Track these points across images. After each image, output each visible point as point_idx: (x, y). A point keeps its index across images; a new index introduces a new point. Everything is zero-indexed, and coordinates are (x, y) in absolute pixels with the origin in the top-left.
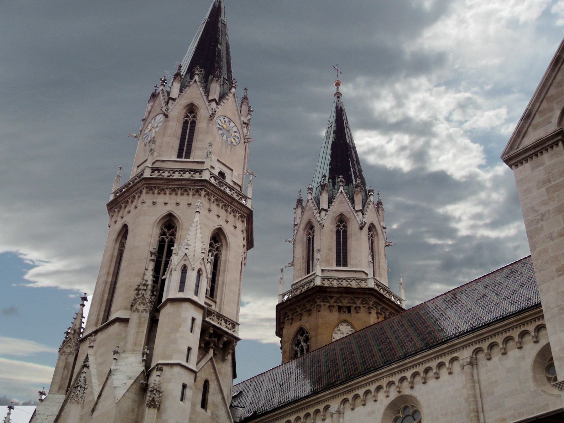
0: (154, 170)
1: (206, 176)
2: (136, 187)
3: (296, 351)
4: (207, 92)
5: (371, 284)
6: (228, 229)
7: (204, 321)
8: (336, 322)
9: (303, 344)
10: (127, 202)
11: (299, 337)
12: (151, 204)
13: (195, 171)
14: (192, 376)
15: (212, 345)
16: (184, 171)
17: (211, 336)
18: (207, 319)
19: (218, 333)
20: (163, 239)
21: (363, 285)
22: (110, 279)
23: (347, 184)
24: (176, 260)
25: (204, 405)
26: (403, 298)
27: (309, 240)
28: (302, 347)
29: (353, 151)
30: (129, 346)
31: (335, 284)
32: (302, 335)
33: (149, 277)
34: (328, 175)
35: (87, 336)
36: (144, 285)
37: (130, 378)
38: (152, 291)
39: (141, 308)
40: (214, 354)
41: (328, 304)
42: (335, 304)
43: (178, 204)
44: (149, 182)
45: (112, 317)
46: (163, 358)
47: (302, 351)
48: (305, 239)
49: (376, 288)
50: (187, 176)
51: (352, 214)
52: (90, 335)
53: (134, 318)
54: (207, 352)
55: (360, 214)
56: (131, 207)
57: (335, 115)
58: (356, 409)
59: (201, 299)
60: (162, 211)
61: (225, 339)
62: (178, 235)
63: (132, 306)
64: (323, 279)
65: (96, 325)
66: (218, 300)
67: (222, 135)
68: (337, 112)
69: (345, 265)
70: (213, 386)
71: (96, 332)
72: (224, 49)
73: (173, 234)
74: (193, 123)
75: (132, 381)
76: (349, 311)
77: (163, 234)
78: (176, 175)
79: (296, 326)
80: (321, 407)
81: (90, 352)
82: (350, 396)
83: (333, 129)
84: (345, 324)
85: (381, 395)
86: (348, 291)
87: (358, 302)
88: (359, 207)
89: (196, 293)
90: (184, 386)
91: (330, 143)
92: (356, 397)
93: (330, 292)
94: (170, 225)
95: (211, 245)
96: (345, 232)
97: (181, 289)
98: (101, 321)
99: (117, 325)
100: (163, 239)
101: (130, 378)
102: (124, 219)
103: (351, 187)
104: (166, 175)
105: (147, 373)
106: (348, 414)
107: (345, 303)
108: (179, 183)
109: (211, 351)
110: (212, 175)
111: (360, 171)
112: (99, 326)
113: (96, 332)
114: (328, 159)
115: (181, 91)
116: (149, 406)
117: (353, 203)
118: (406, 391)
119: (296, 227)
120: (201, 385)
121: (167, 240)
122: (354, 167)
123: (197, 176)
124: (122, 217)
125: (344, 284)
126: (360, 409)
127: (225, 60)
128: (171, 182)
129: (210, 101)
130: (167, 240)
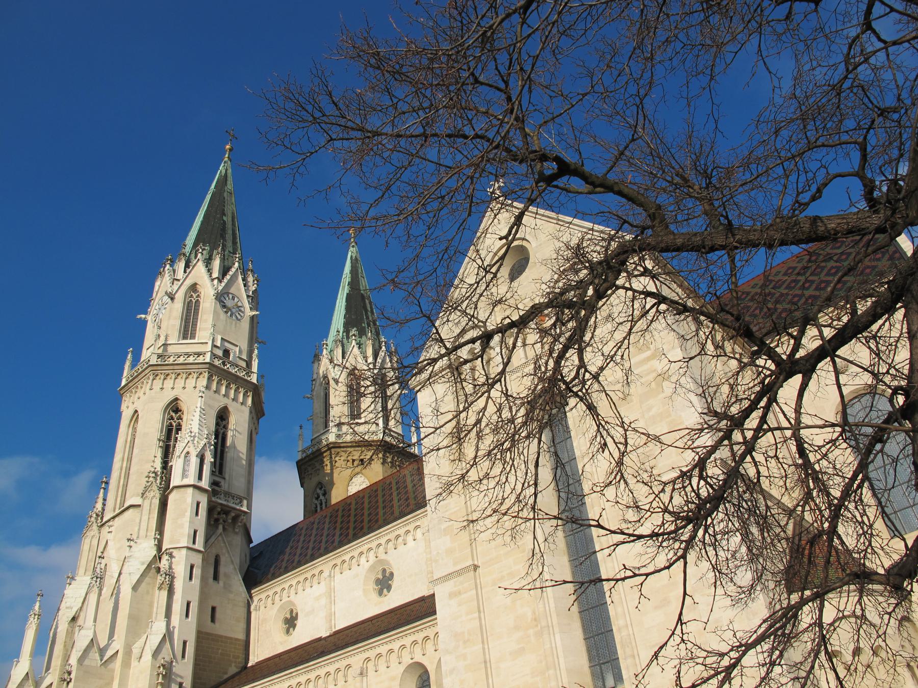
0: (159, 356)
1: (208, 360)
4: (210, 271)
6: (233, 407)
7: (209, 502)
9: (322, 497)
10: (137, 387)
11: (318, 491)
12: (159, 390)
13: (199, 354)
14: (200, 556)
15: (221, 521)
16: (188, 355)
17: (219, 513)
18: (213, 499)
19: (226, 511)
23: (360, 337)
24: (180, 446)
25: (216, 577)
30: (143, 532)
33: (158, 466)
34: (341, 330)
35: (106, 522)
36: (154, 472)
37: (143, 564)
38: (162, 478)
39: (152, 494)
40: (224, 529)
41: (342, 458)
42: (349, 458)
43: (184, 388)
44: (155, 368)
45: (127, 505)
46: (171, 542)
47: (321, 504)
48: (322, 394)
50: (191, 359)
52: (109, 520)
54: (217, 528)
56: (140, 393)
59: (205, 483)
60: (168, 396)
61: (233, 514)
62: (184, 419)
63: (143, 494)
65: (114, 511)
66: (227, 477)
67: (227, 312)
70: (223, 560)
71: (114, 518)
72: (230, 219)
73: (180, 418)
74: (198, 302)
78: (181, 360)
79: (315, 480)
80: (316, 572)
81: (110, 536)
82: (338, 561)
85: (363, 559)
89: (200, 478)
90: (192, 567)
92: (344, 562)
93: (344, 447)
95: (217, 424)
98: (118, 506)
99: (131, 510)
100: (171, 425)
102: (135, 405)
103: (364, 338)
105: (158, 557)
106: (338, 576)
107: (356, 455)
109: (221, 527)
110: (214, 356)
112: (117, 511)
113: (114, 518)
114: (343, 312)
115: (185, 272)
116: (160, 588)
118: (382, 556)
120: (212, 561)
122: (367, 318)
123: (200, 359)
126: (347, 573)
127: (230, 232)
128: (176, 367)
129: (213, 280)
130: (174, 424)
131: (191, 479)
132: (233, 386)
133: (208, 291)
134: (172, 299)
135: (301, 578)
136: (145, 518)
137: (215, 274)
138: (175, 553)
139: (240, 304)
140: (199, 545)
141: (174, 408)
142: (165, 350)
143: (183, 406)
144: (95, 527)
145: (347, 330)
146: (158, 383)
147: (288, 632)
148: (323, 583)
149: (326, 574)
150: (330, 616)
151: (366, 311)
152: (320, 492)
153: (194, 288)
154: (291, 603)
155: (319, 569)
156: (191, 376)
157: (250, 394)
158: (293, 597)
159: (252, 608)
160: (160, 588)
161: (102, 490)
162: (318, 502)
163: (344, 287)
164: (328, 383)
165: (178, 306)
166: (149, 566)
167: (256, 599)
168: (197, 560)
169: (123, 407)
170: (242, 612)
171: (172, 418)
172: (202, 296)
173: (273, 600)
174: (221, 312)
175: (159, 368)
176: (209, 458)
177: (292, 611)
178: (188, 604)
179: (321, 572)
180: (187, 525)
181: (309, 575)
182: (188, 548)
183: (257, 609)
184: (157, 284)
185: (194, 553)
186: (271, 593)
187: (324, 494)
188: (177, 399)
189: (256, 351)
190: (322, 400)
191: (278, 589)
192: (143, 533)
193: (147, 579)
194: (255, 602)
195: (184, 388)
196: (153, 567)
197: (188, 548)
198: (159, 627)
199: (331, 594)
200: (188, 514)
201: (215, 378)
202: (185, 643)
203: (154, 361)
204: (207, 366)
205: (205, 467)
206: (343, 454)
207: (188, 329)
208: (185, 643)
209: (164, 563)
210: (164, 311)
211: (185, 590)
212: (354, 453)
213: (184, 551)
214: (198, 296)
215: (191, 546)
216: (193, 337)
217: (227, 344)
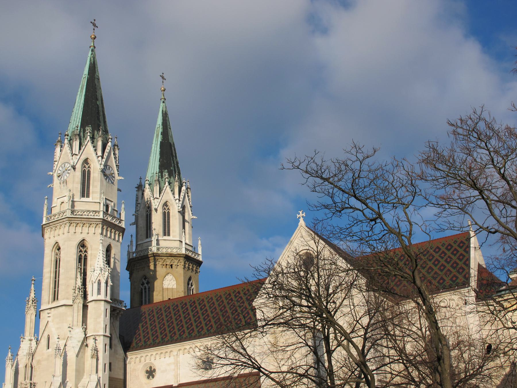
0: (73, 212)
1: (101, 217)
2: (62, 221)
3: (142, 289)
5: (183, 252)
6: (114, 244)
8: (165, 274)
11: (144, 281)
13: (96, 212)
20: (81, 255)
21: (179, 252)
22: (52, 275)
23: (170, 178)
26: (200, 252)
27: (147, 215)
28: (145, 287)
29: (173, 148)
30: (75, 323)
31: (164, 251)
32: (145, 279)
37: (79, 342)
41: (160, 263)
43: (88, 233)
44: (70, 219)
47: (145, 289)
48: (145, 215)
49: (187, 253)
50: (91, 215)
51: (174, 201)
53: (75, 306)
55: (177, 201)
57: (162, 118)
58: (185, 355)
59: (108, 299)
62: (89, 252)
64: (158, 249)
68: (163, 116)
69: (169, 235)
73: (86, 251)
74: (89, 172)
75: (80, 343)
76: (172, 267)
77: (81, 251)
80: (169, 350)
81: (49, 319)
82: (183, 348)
83: (161, 130)
84: (169, 275)
86: (171, 255)
87: (176, 261)
88: (177, 196)
91: (159, 143)
92: (185, 349)
94: (84, 245)
96: (169, 213)
97: (99, 293)
98: (51, 301)
99: (64, 307)
100: (81, 255)
101: (79, 342)
103: (172, 179)
104: (79, 213)
105: (86, 338)
106: (181, 355)
108: (88, 220)
111: (177, 163)
114: (158, 156)
115: (80, 149)
117: (173, 194)
119: (139, 205)
121: (83, 255)
122: (174, 162)
124: (54, 237)
125: (169, 251)
128: (83, 220)
129: (98, 157)
130: (83, 255)
131: (102, 297)
132: (113, 231)
133: (96, 166)
134: (74, 168)
135: (159, 352)
136: (76, 314)
137: (100, 153)
138: (97, 338)
139: (112, 172)
140: (108, 334)
141: (82, 245)
142: (73, 206)
143: (88, 244)
144: (32, 308)
145: (161, 172)
146: (72, 229)
147: (148, 378)
148: (172, 357)
149: (175, 353)
150: (177, 376)
151: (173, 156)
152: (145, 282)
153: (86, 161)
154: (153, 364)
155: (170, 350)
156: (91, 226)
157: (121, 234)
158: (153, 361)
159: (128, 362)
160: (92, 357)
161: (33, 285)
162: (143, 288)
163: (157, 135)
164: (151, 211)
165: (78, 174)
166: (83, 343)
167: (129, 357)
168: (108, 341)
169: (46, 236)
170: (122, 364)
171: (81, 251)
172: (92, 166)
173: (140, 360)
174: (103, 179)
175: (73, 219)
176: (110, 283)
177: (151, 367)
178: (105, 364)
179: (171, 351)
180: (102, 323)
181: (164, 351)
182: (104, 336)
183: (130, 363)
184: (58, 149)
185: (106, 338)
186: (139, 356)
187: (148, 283)
188: (84, 240)
189: (123, 206)
190: (145, 218)
191: (144, 355)
192: (75, 323)
193: (82, 350)
194: (128, 360)
195: (88, 233)
196: (84, 344)
197: (104, 336)
198: (94, 378)
199: (177, 364)
200: (103, 316)
201: (105, 227)
202: (105, 385)
203: (68, 214)
204: (101, 220)
205: (108, 288)
206: (160, 260)
207: (85, 192)
208: (105, 385)
209: (91, 342)
210: (68, 175)
211: (103, 357)
212: (167, 260)
213: (102, 337)
214: (89, 167)
215: (105, 334)
216: (88, 196)
217: (108, 202)
